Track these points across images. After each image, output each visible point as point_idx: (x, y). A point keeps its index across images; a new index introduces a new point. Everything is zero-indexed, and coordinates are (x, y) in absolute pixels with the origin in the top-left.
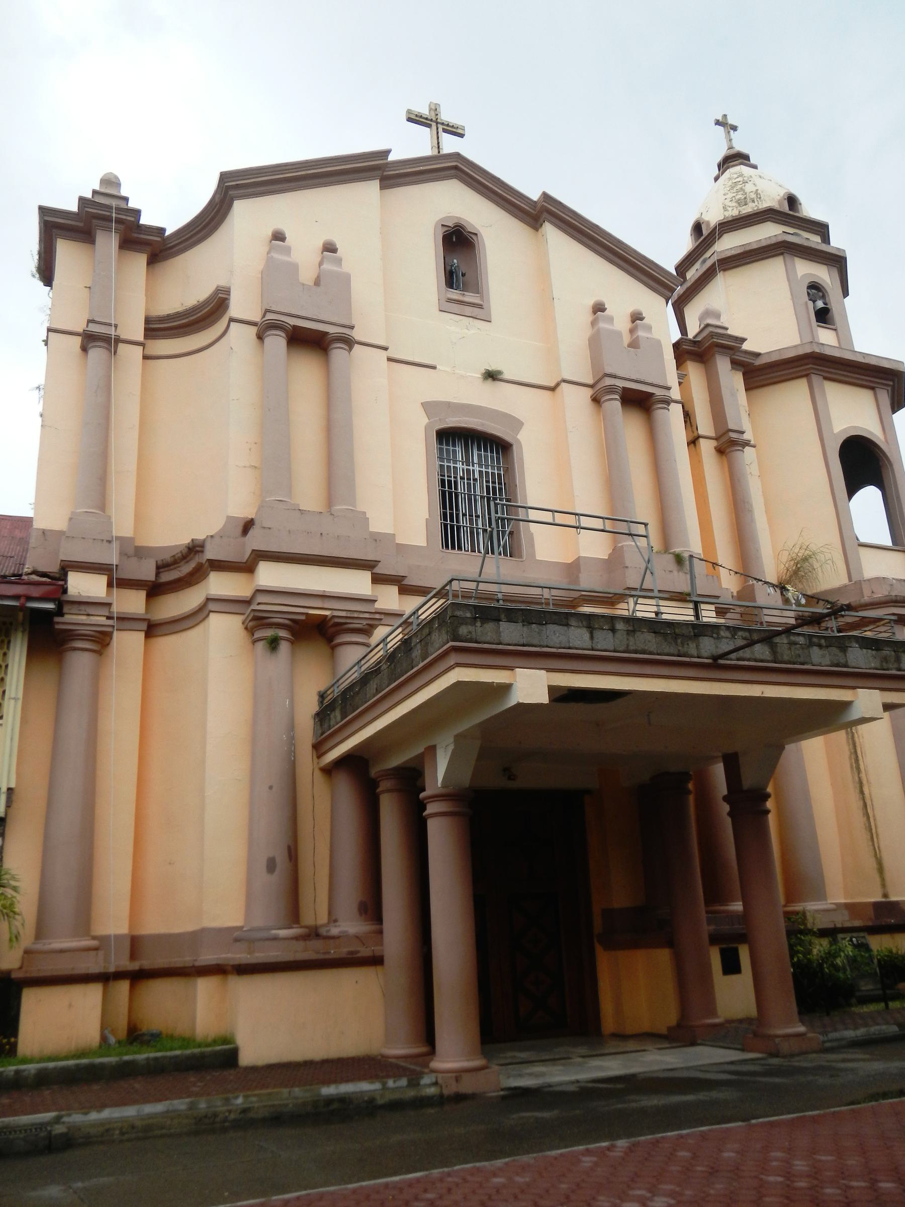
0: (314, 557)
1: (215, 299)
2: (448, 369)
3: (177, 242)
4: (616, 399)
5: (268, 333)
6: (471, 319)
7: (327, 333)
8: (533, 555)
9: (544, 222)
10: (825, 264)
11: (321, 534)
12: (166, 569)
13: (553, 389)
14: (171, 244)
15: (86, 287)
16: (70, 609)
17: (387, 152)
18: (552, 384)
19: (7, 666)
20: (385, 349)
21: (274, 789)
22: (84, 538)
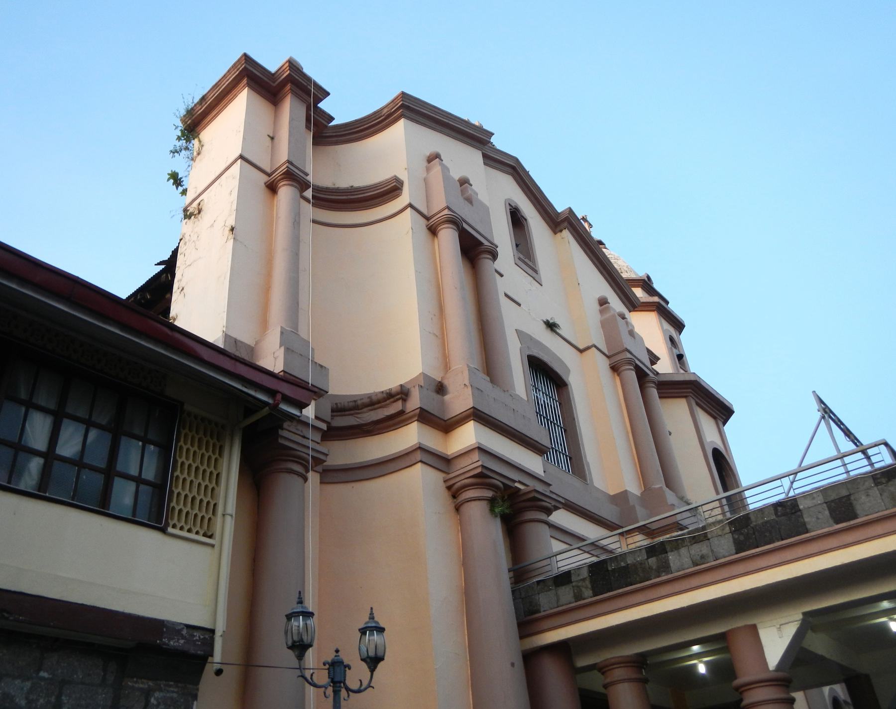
0: (511, 429)
1: (385, 187)
2: (527, 310)
3: (331, 134)
4: (632, 369)
5: (440, 228)
6: (532, 279)
7: (481, 244)
8: (591, 480)
9: (565, 229)
10: (674, 327)
11: (514, 410)
12: (339, 414)
13: (581, 351)
14: (327, 134)
15: (269, 136)
16: (289, 426)
17: (491, 134)
18: (581, 347)
19: (218, 475)
20: (502, 275)
21: (515, 665)
22: (301, 355)
